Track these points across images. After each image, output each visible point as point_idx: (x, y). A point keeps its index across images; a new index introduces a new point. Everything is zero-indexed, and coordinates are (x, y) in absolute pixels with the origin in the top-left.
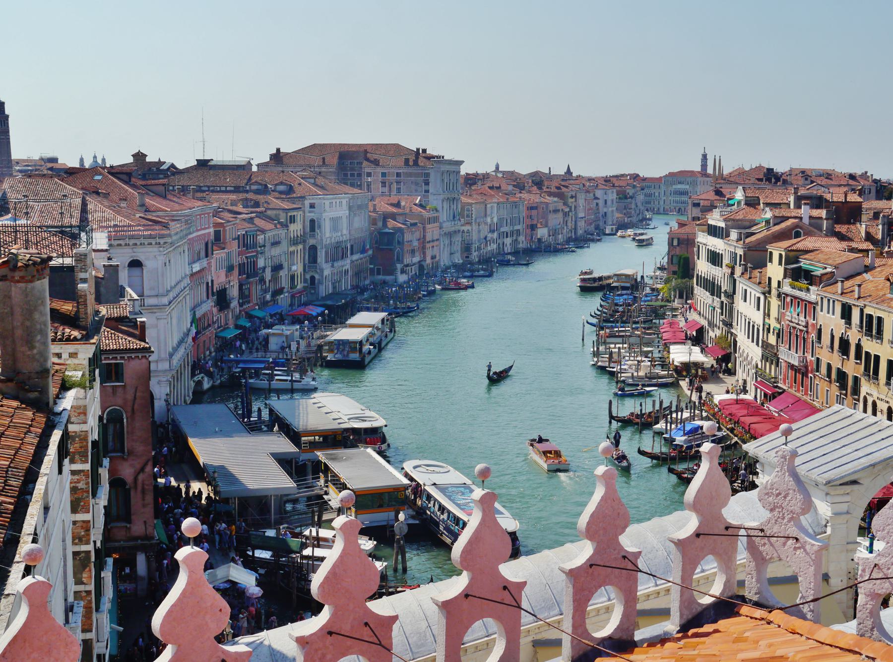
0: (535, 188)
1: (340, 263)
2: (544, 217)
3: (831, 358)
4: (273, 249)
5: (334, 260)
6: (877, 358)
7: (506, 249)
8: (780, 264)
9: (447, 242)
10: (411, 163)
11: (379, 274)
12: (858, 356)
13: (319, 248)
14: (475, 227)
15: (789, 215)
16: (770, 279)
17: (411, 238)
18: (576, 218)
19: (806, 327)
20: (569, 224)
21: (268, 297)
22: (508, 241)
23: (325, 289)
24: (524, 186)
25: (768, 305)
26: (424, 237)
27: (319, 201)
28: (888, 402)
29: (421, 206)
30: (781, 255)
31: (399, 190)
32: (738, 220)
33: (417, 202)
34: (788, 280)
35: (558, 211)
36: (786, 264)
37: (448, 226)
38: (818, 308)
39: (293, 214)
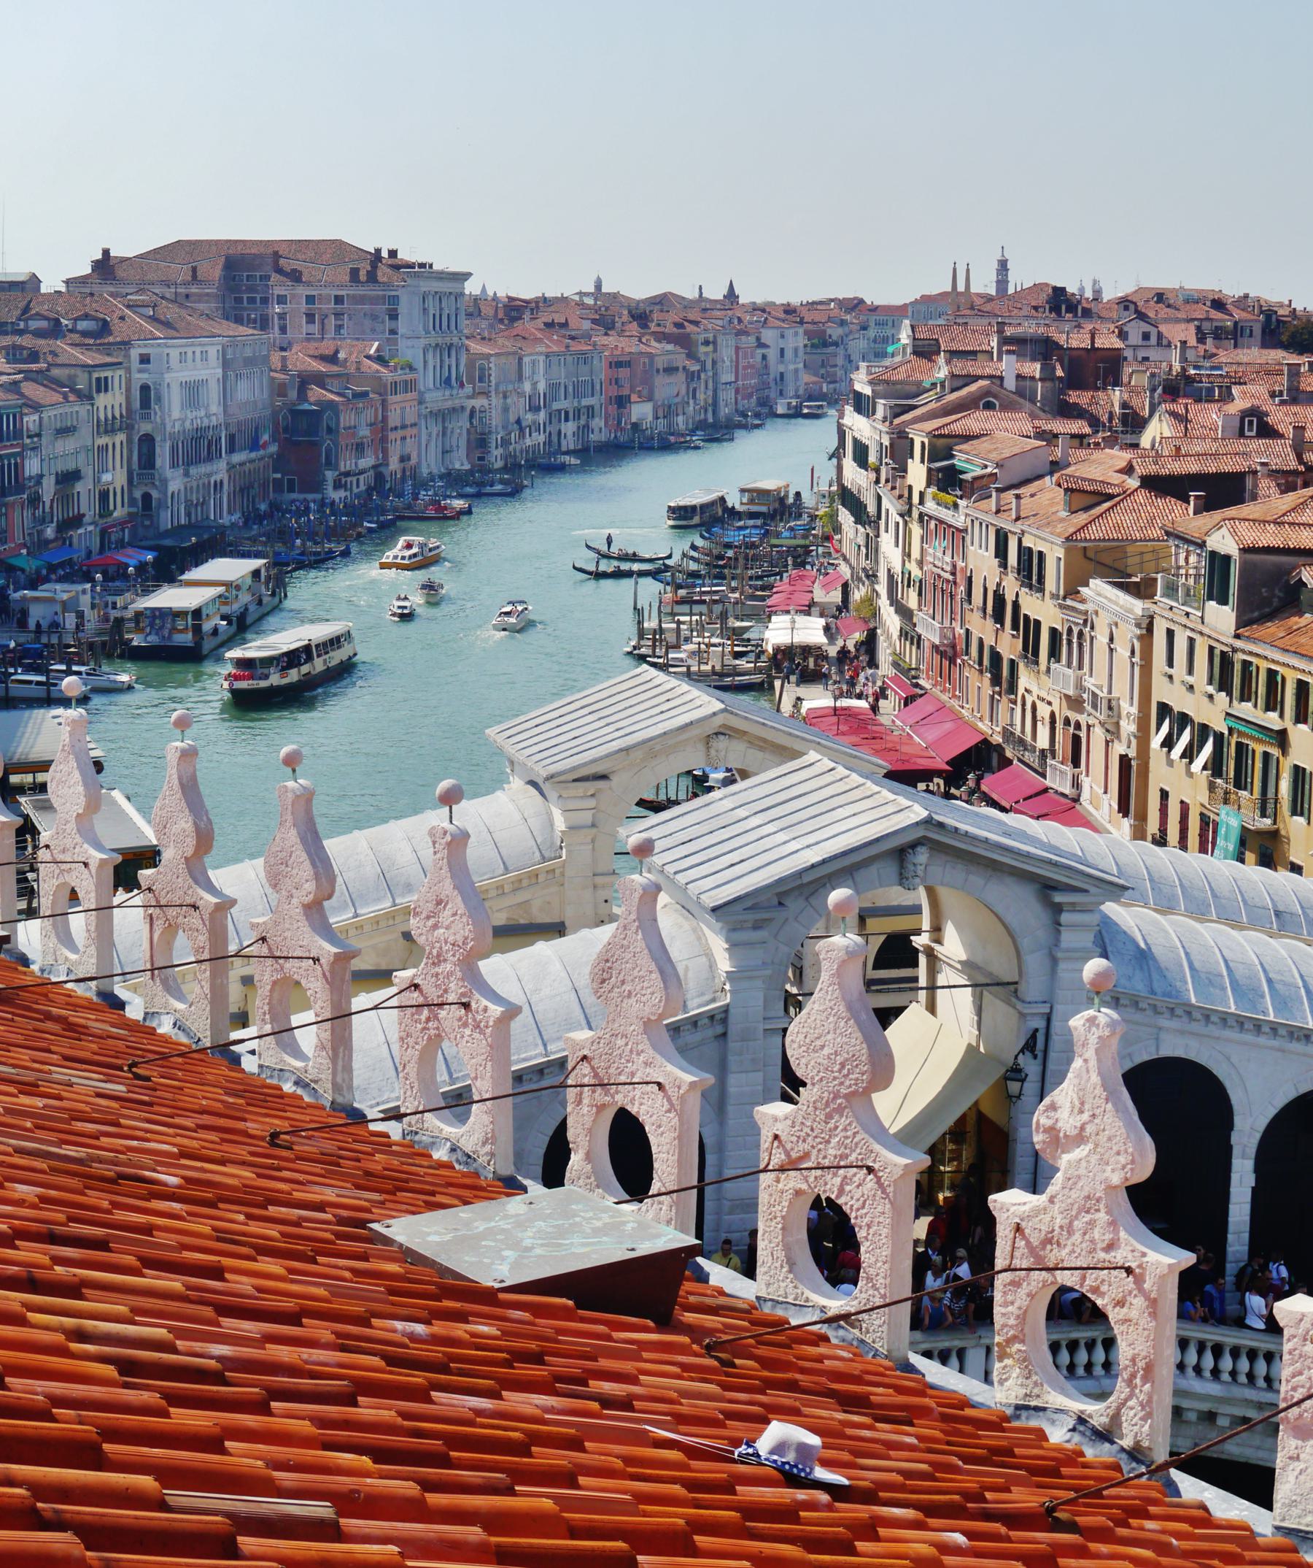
0: (634, 328)
1: (203, 469)
2: (647, 380)
3: (982, 628)
4: (59, 443)
5: (189, 463)
6: (1037, 623)
7: (564, 443)
8: (923, 462)
9: (435, 429)
11: (291, 490)
12: (1015, 626)
13: (158, 439)
14: (494, 400)
15: (979, 373)
16: (910, 487)
17: (357, 421)
18: (715, 383)
19: (953, 574)
20: (701, 396)
21: (50, 532)
22: (569, 428)
23: (165, 520)
24: (613, 322)
25: (908, 533)
26: (385, 419)
27: (158, 350)
28: (1050, 703)
29: (380, 359)
30: (923, 443)
31: (339, 328)
32: (895, 383)
33: (372, 352)
34: (933, 490)
35: (677, 369)
36: (931, 460)
37: (437, 399)
38: (968, 539)
39: (103, 375)
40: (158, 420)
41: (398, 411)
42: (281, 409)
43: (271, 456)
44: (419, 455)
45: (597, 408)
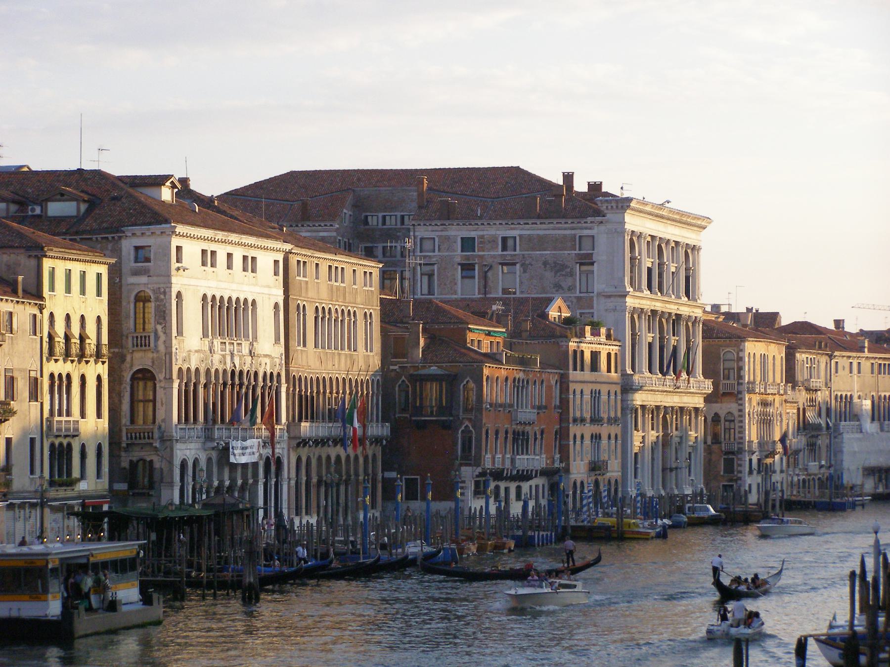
13: (160, 376)
26: (564, 404)
40: (162, 348)
41: (587, 397)
42: (398, 375)
43: (377, 440)
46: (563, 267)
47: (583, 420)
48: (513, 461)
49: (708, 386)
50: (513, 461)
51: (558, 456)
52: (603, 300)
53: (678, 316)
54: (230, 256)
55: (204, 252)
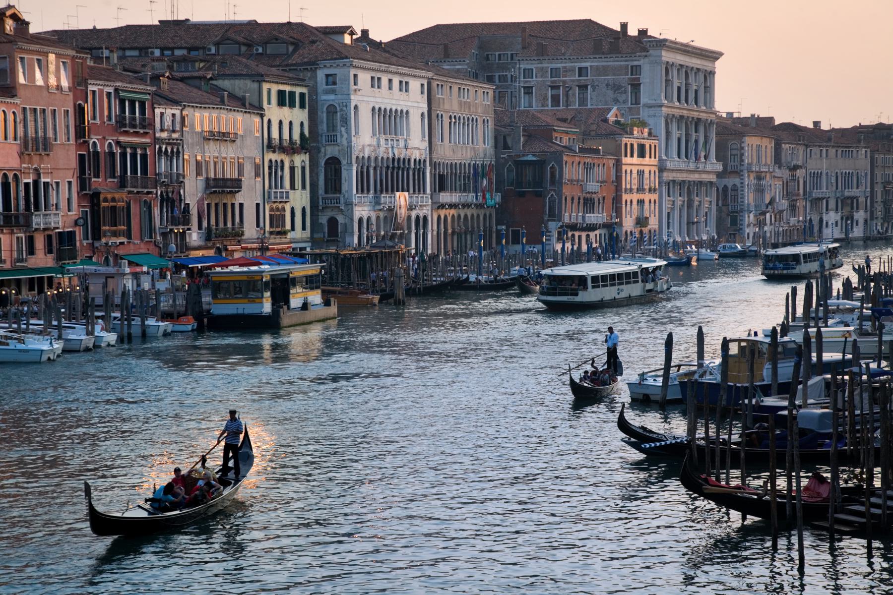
5: (379, 191)
10: (606, 47)
13: (344, 162)
26: (619, 179)
40: (345, 143)
41: (635, 175)
42: (506, 161)
44: (660, 221)
45: (862, 200)
46: (620, 87)
47: (631, 190)
48: (583, 217)
49: (719, 167)
50: (583, 217)
51: (614, 214)
52: (646, 109)
53: (699, 120)
54: (390, 81)
55: (373, 78)
